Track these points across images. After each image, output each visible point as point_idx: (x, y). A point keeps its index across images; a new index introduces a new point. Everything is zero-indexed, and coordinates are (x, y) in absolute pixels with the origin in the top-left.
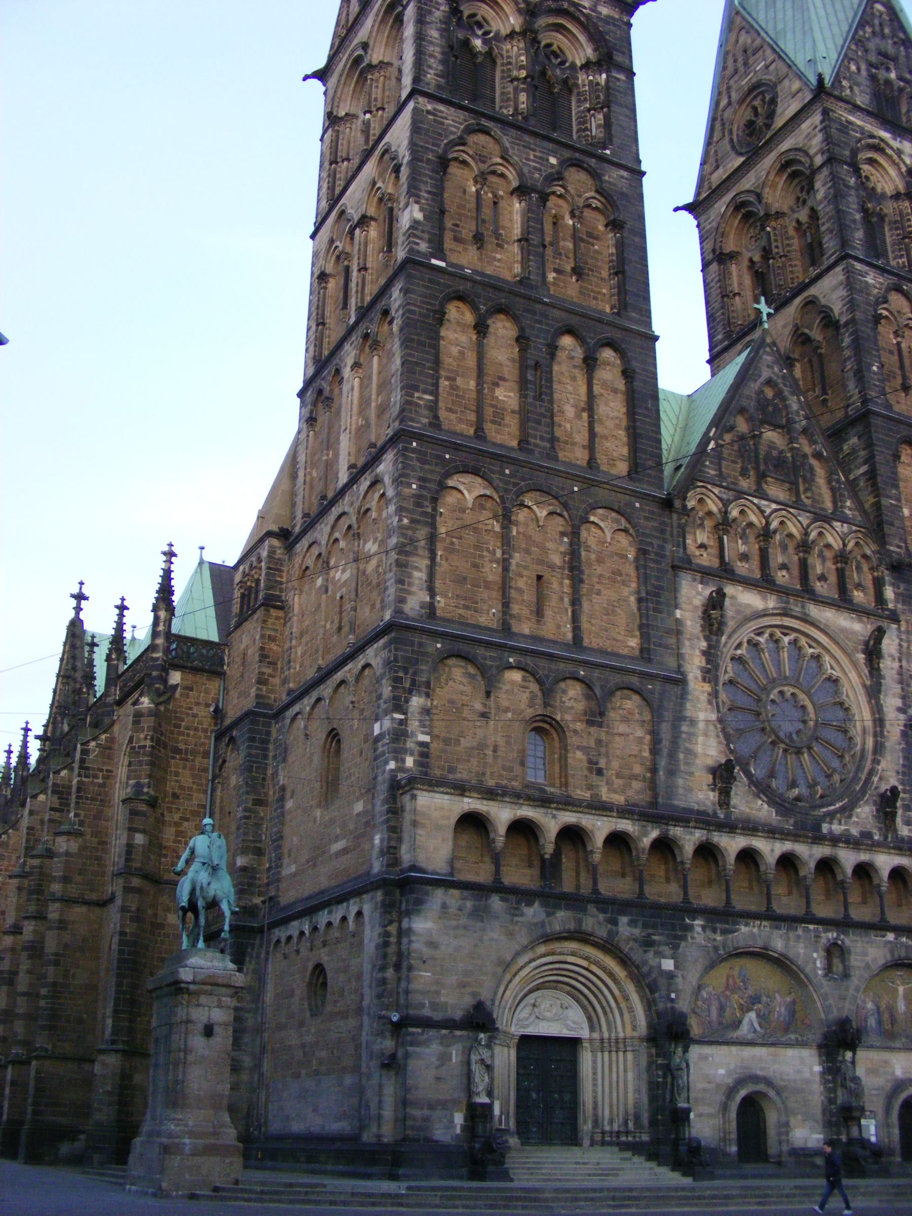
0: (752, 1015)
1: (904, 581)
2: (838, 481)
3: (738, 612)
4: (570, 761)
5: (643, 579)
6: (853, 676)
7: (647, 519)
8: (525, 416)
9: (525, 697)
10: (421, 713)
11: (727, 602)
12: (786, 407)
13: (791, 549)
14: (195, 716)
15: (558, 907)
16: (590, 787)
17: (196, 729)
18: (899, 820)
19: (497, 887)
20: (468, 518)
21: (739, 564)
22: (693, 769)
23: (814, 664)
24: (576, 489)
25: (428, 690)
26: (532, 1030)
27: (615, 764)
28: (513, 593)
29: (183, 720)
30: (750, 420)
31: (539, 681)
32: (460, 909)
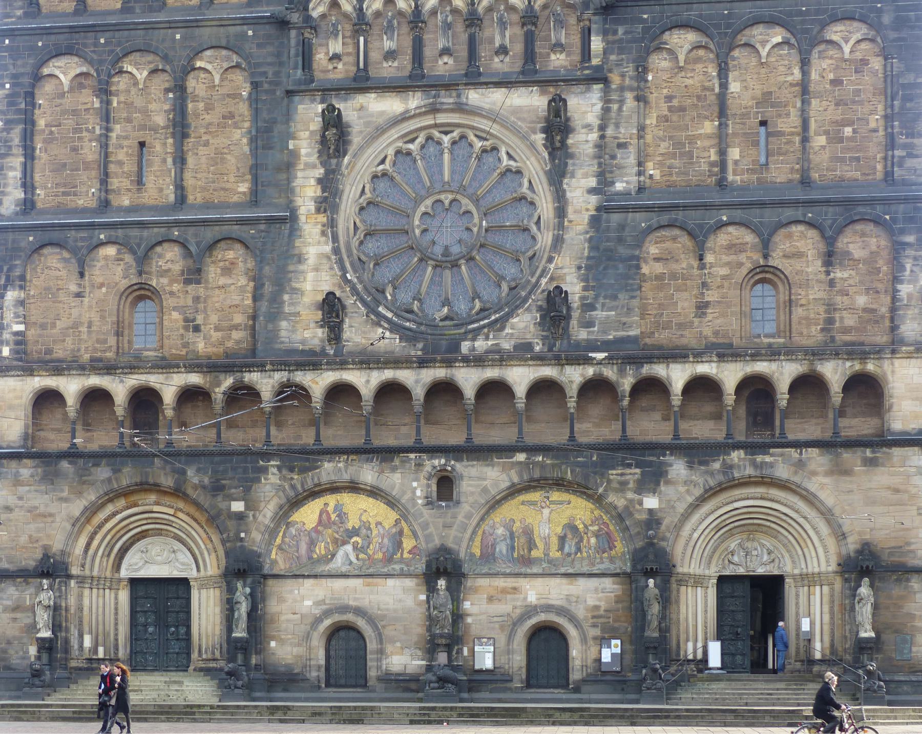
0: (349, 548)
3: (367, 124)
4: (165, 323)
7: (259, 46)
9: (119, 270)
10: (15, 306)
13: (460, 27)
18: (574, 323)
20: (68, 102)
21: (385, 65)
22: (299, 309)
24: (178, 37)
27: (214, 318)
28: (112, 168)
31: (133, 252)
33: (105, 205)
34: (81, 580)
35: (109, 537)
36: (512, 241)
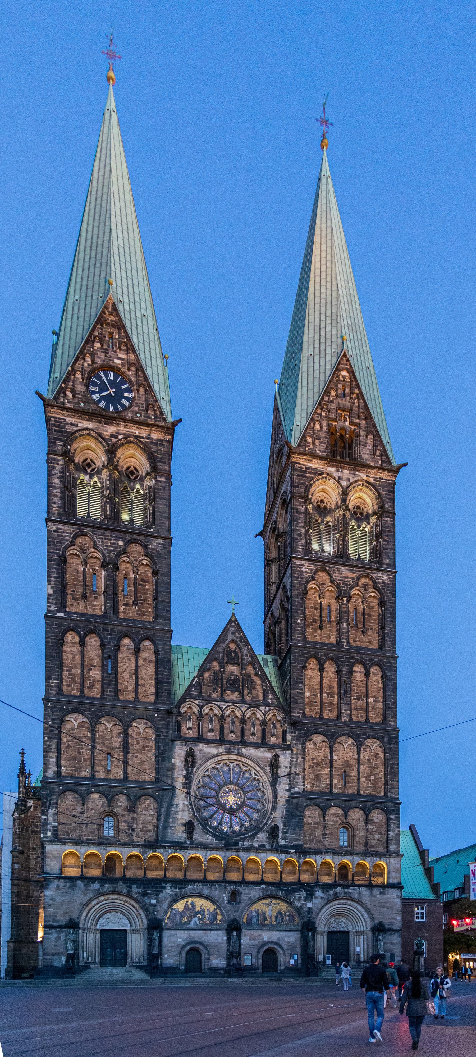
0: (196, 919)
1: (298, 730)
2: (266, 686)
3: (203, 756)
5: (158, 748)
7: (160, 720)
8: (104, 682)
9: (100, 804)
12: (241, 652)
13: (237, 723)
18: (280, 839)
24: (126, 712)
27: (140, 826)
28: (96, 762)
30: (220, 663)
31: (106, 797)
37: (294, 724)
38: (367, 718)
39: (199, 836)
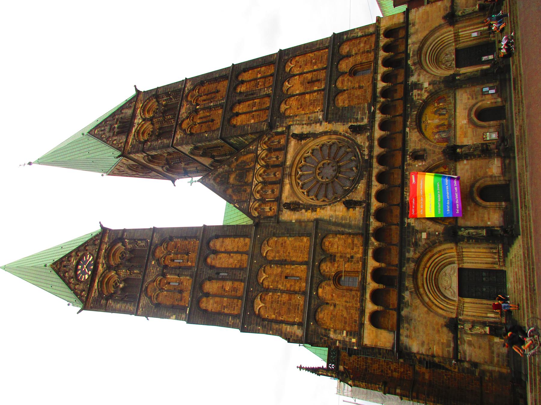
1: (275, 123)
2: (244, 152)
3: (291, 196)
4: (349, 270)
5: (283, 235)
6: (310, 145)
7: (263, 233)
8: (234, 280)
9: (327, 288)
11: (288, 201)
12: (222, 173)
13: (269, 171)
14: (353, 362)
15: (404, 284)
16: (358, 262)
17: (358, 361)
18: (362, 124)
19: (399, 310)
20: (268, 305)
23: (308, 160)
25: (327, 330)
26: (456, 290)
27: (349, 250)
28: (292, 289)
29: (355, 366)
31: (321, 282)
32: (408, 329)
33: (304, 293)
34: (458, 314)
35: (438, 300)
36: (334, 149)
37: (271, 126)
38: (272, 75)
39: (359, 195)
